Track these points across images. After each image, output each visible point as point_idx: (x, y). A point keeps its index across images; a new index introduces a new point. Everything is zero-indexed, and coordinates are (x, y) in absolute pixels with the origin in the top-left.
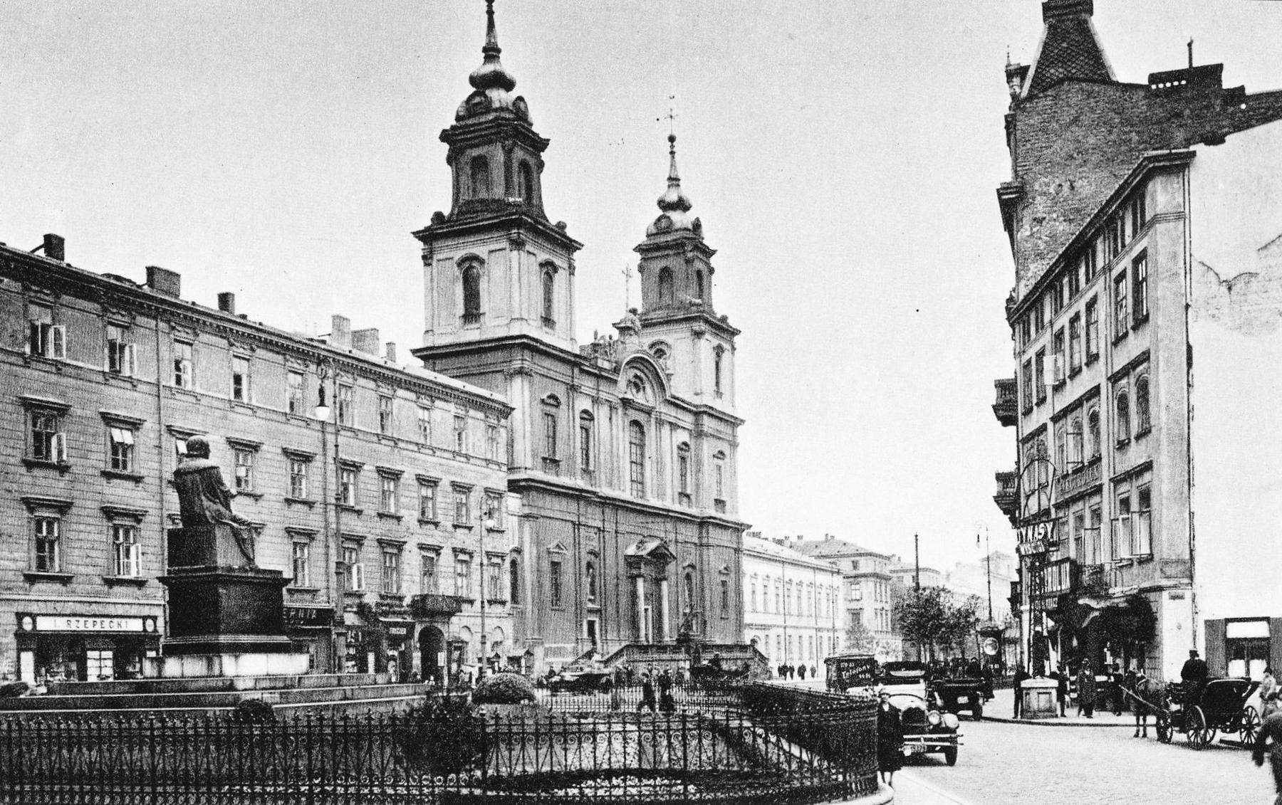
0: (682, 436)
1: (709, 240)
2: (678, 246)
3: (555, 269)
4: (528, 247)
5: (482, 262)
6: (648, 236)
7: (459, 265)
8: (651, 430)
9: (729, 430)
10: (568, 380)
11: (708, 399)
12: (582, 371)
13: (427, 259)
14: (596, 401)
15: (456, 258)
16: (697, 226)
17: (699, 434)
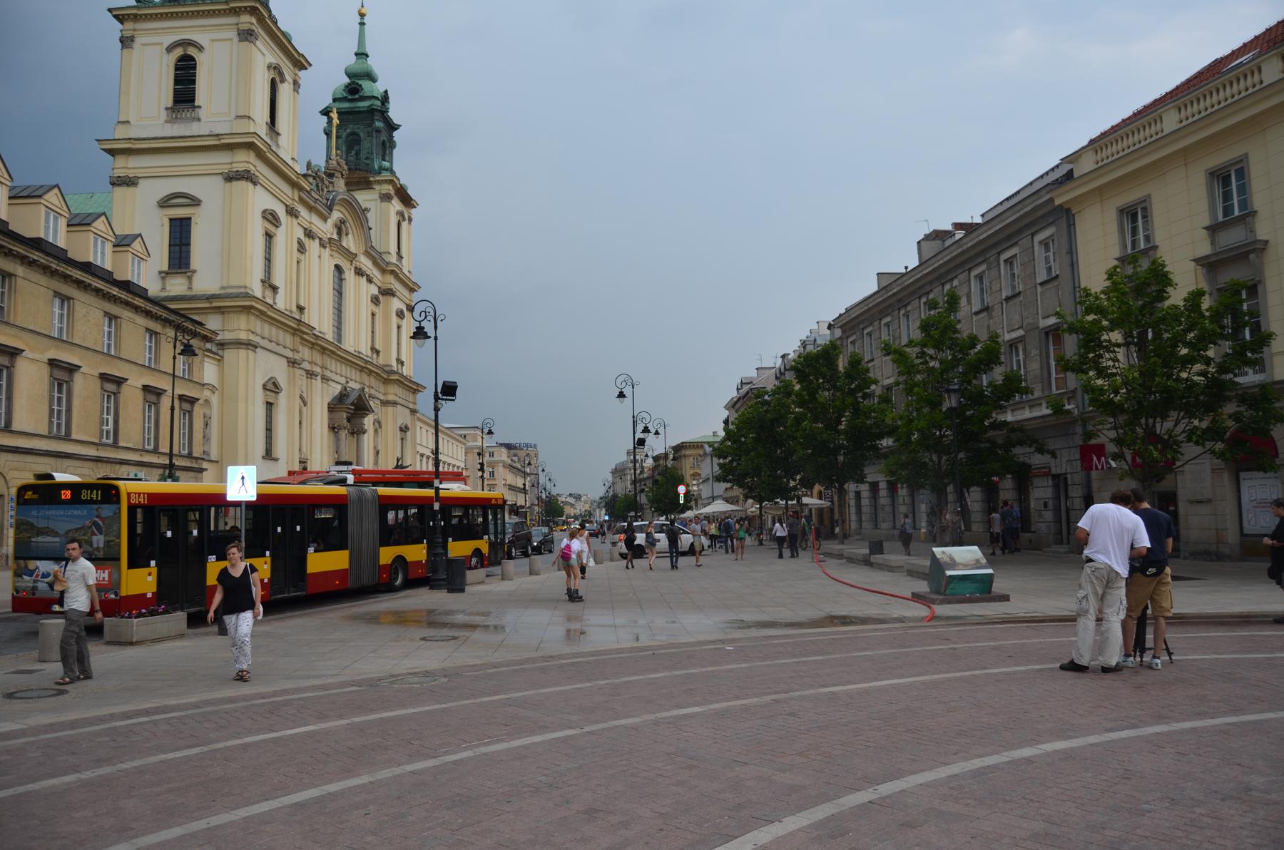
0: (374, 290)
1: (394, 114)
2: (371, 111)
3: (283, 80)
4: (258, 43)
5: (200, 48)
6: (335, 100)
7: (170, 49)
8: (349, 275)
9: (406, 293)
10: (289, 202)
11: (393, 259)
12: (301, 200)
13: (126, 42)
14: (309, 234)
15: (166, 45)
16: (385, 98)
17: (388, 293)
